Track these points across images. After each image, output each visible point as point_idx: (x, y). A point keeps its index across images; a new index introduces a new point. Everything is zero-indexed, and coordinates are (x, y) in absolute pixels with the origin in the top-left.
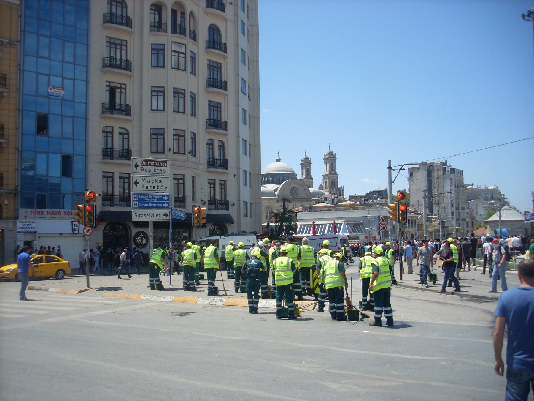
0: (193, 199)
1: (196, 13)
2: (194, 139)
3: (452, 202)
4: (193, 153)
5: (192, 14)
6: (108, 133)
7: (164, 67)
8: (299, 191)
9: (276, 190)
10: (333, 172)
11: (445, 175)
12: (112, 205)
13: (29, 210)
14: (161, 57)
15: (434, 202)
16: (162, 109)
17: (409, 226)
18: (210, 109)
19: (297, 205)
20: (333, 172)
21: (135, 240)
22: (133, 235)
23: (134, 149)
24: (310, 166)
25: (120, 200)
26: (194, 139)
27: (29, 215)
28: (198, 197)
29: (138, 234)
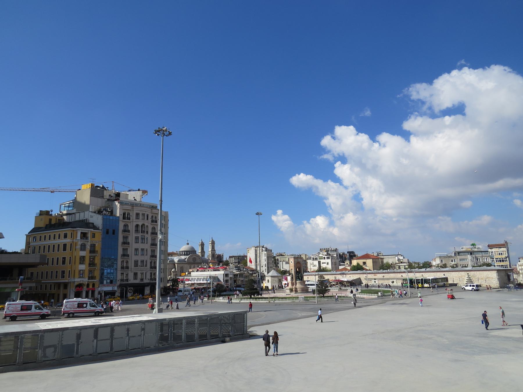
0: (146, 279)
1: (148, 225)
2: (146, 262)
3: (265, 264)
4: (146, 266)
5: (147, 226)
6: (122, 262)
7: (138, 243)
8: (197, 259)
9: (186, 259)
10: (213, 250)
11: (263, 252)
12: (123, 282)
13: (102, 285)
14: (138, 240)
15: (258, 264)
16: (137, 254)
17: (239, 277)
18: (151, 252)
19: (195, 265)
20: (213, 250)
21: (129, 291)
22: (129, 289)
23: (129, 266)
24: (204, 246)
25: (125, 280)
26: (146, 262)
27: (102, 286)
28: (147, 278)
29: (130, 289)
